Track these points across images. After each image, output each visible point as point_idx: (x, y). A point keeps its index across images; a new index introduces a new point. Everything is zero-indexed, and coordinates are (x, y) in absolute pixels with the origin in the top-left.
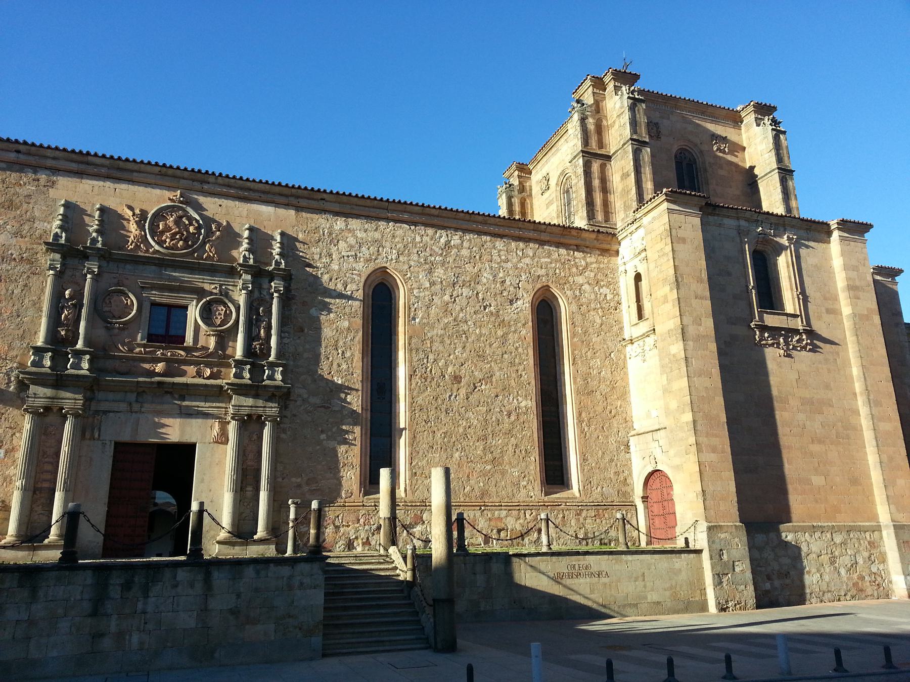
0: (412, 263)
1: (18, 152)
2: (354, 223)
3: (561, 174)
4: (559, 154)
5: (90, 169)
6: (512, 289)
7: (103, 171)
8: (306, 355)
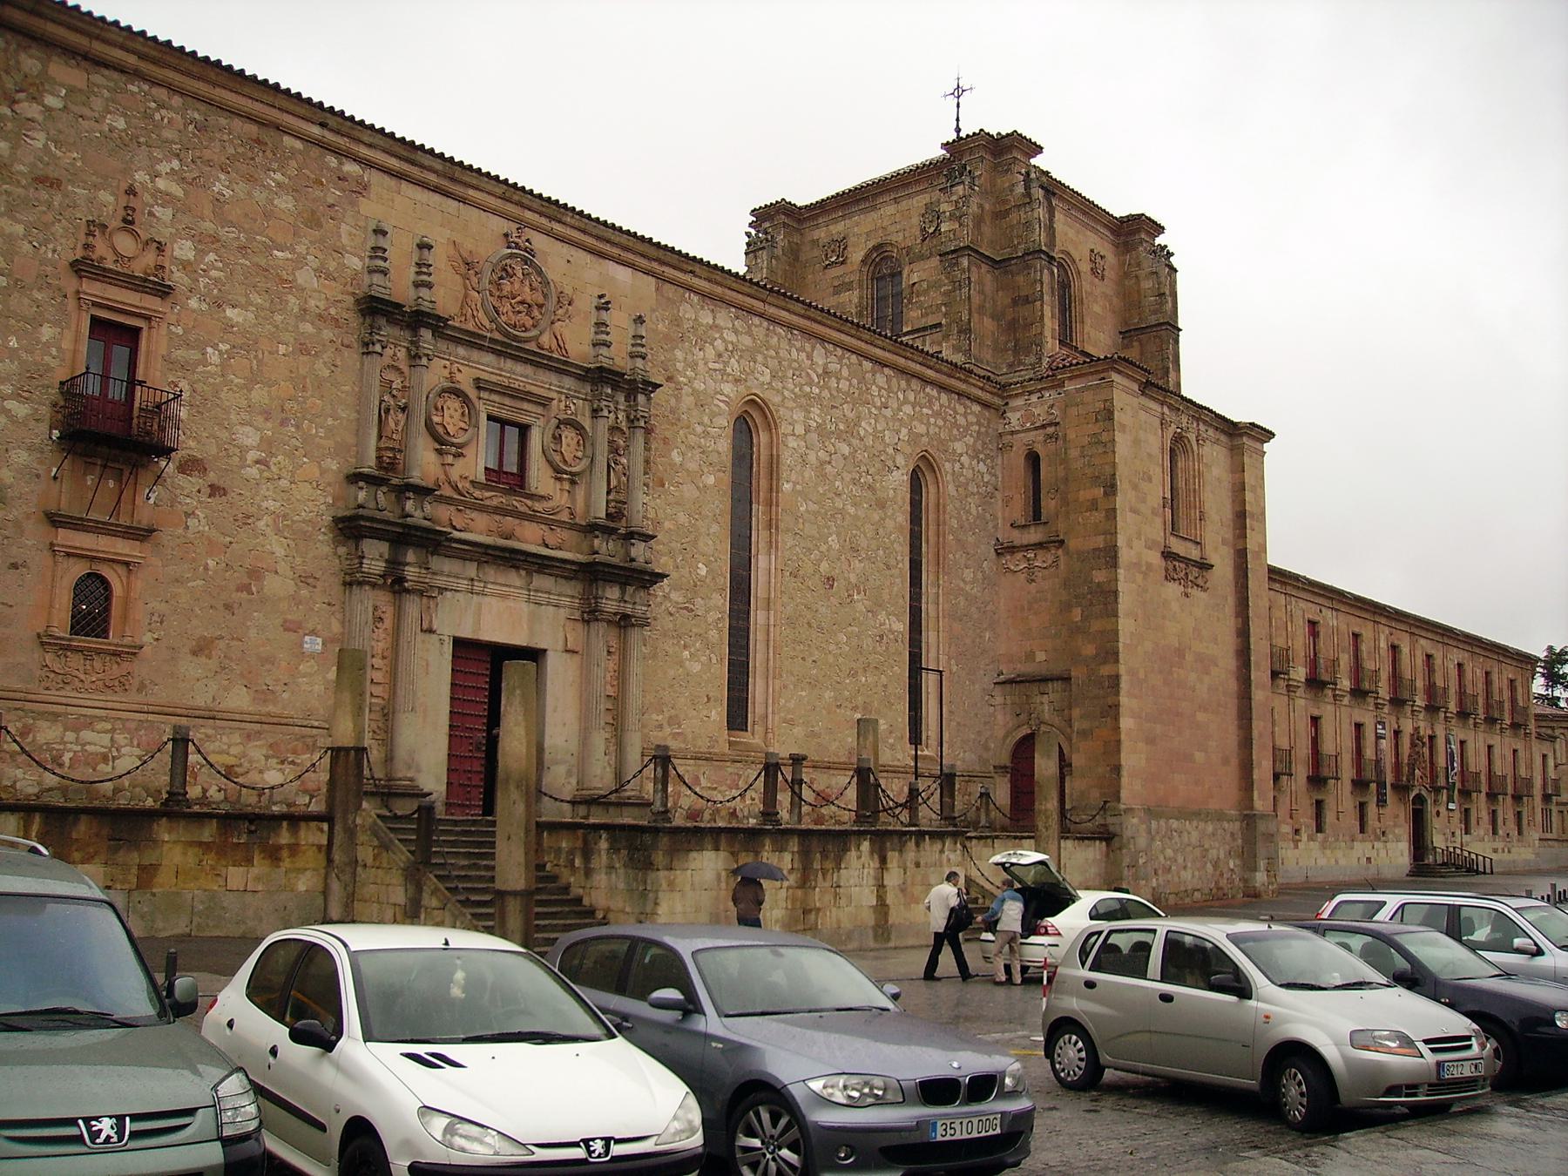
0: (786, 393)
1: (323, 125)
2: (724, 317)
3: (875, 248)
4: (874, 215)
5: (414, 171)
6: (890, 450)
7: (432, 178)
8: (667, 525)
